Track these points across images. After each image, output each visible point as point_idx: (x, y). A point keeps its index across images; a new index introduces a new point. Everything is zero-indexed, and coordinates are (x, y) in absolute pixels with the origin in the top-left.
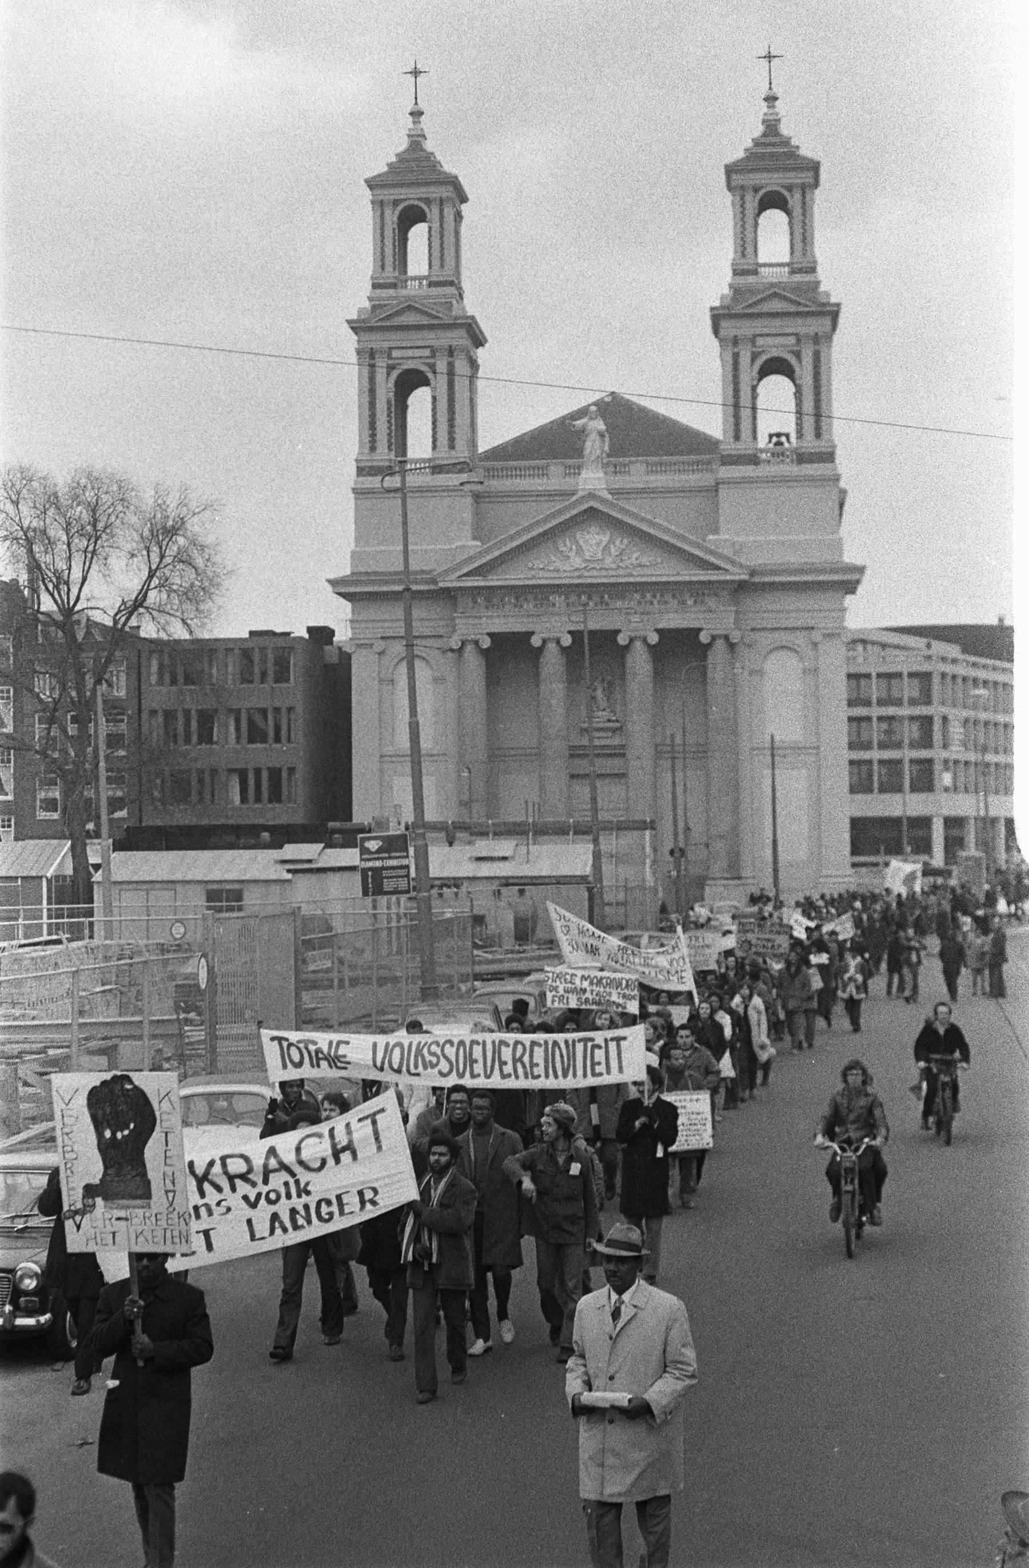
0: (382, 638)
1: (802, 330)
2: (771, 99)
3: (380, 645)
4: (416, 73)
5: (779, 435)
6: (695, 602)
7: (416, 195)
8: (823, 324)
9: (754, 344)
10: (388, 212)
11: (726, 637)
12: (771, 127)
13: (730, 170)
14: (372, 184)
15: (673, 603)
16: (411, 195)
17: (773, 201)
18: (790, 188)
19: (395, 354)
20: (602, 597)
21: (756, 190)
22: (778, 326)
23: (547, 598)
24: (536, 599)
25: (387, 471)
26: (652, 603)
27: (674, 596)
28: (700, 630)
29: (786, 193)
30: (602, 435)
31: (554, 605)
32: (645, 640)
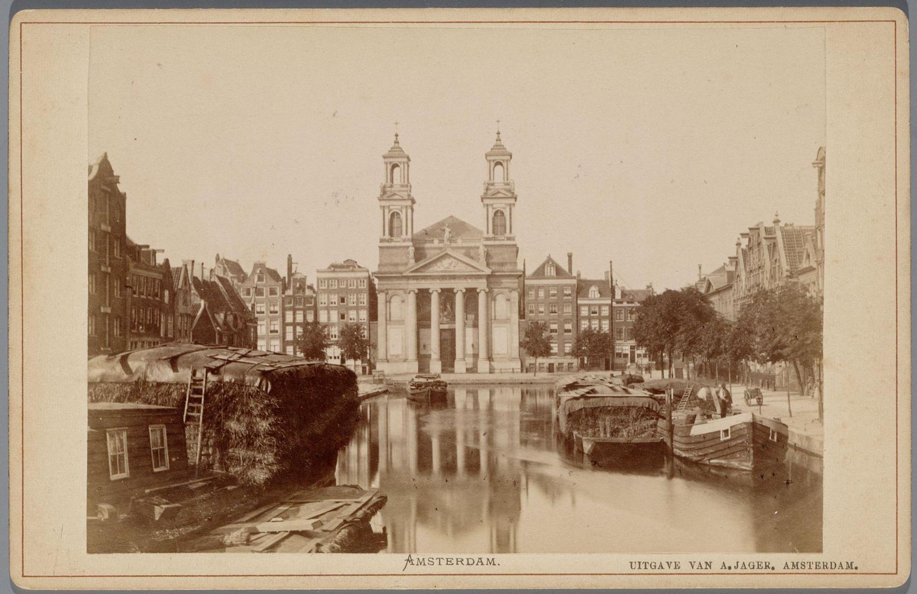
2: (499, 133)
7: (396, 160)
8: (512, 201)
13: (486, 156)
14: (384, 157)
16: (395, 161)
17: (499, 163)
22: (500, 201)
25: (388, 241)
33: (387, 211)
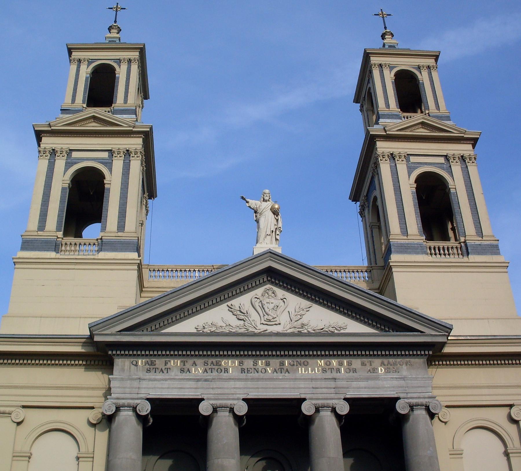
0: (24, 407)
3: (20, 414)
6: (387, 371)
9: (408, 160)
11: (427, 409)
15: (362, 373)
19: (75, 155)
20: (282, 364)
24: (206, 363)
26: (338, 371)
27: (363, 364)
28: (398, 399)
30: (275, 213)
31: (226, 370)
32: (334, 410)
33: (60, 163)
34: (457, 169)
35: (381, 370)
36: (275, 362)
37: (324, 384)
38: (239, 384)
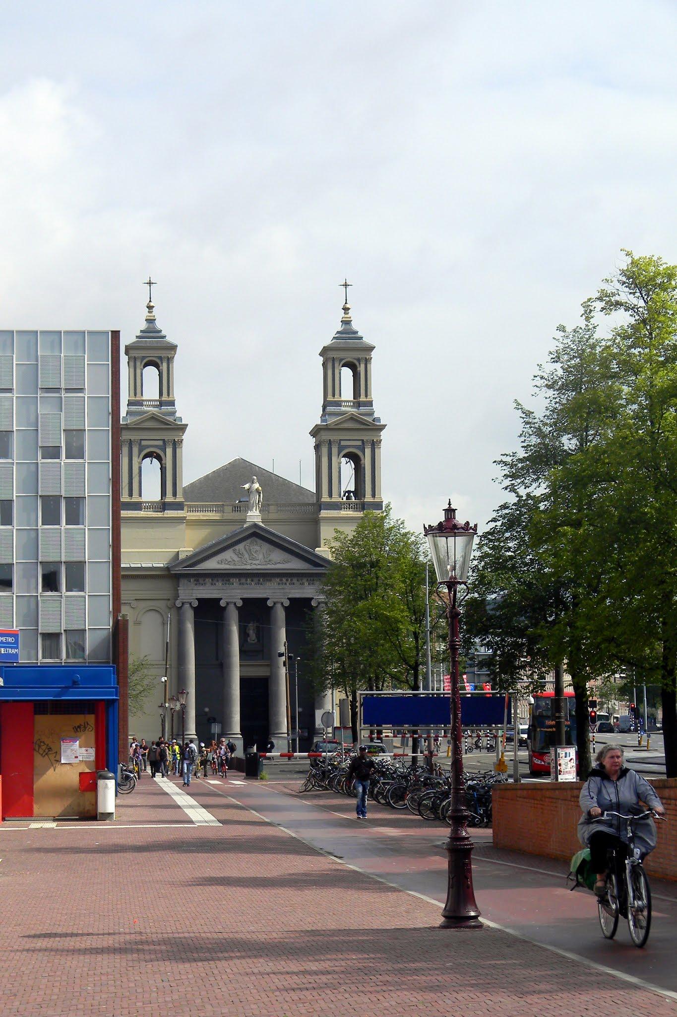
1: (365, 438)
2: (346, 310)
4: (150, 283)
5: (349, 492)
10: (138, 364)
12: (346, 323)
18: (359, 360)
19: (143, 443)
21: (341, 360)
23: (229, 580)
29: (357, 364)
34: (368, 451)
35: (306, 584)
36: (256, 580)
37: (278, 591)
38: (239, 591)
